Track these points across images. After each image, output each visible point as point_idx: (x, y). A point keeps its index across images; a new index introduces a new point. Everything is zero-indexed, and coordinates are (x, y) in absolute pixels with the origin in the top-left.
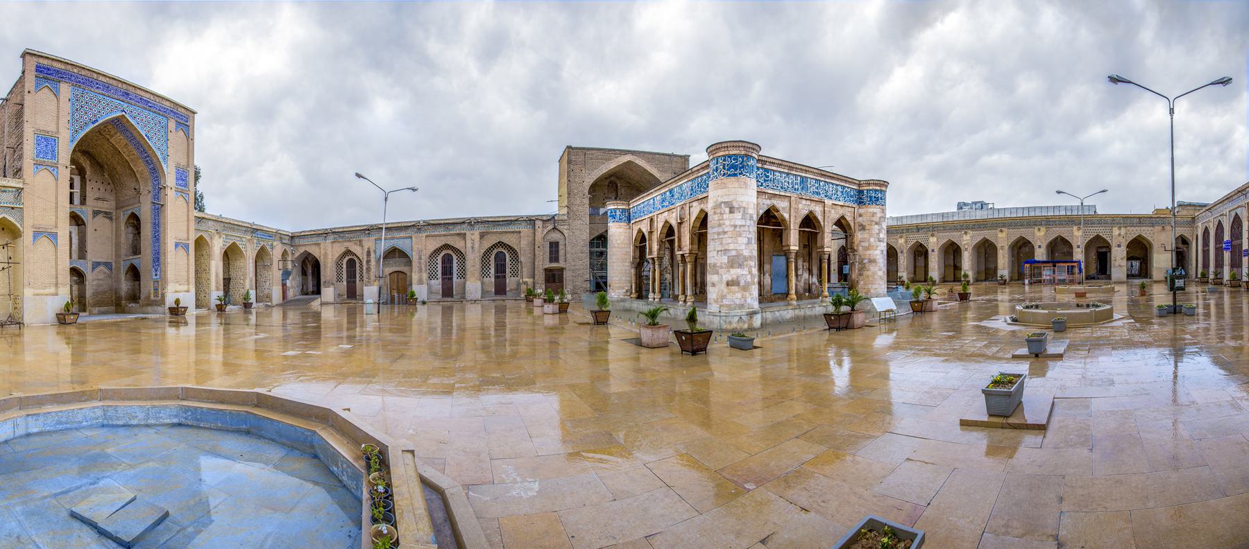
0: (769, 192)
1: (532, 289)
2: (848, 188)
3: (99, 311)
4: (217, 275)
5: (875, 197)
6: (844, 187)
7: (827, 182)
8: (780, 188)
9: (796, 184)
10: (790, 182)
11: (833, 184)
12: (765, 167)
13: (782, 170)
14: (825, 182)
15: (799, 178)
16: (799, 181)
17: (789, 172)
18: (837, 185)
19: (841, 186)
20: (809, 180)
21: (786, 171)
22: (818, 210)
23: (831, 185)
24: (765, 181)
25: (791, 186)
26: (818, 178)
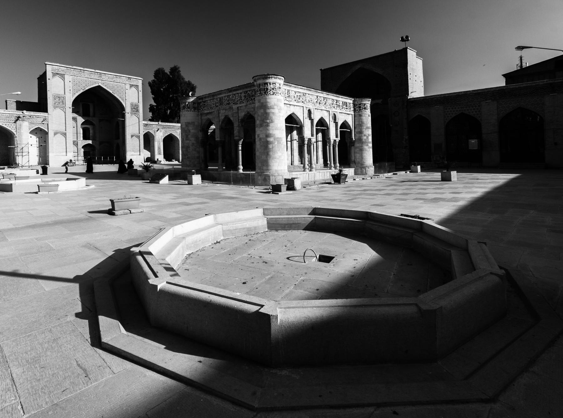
0: (206, 112)
1: (72, 162)
2: (249, 91)
4: (159, 148)
6: (247, 92)
7: (234, 95)
8: (210, 109)
9: (217, 103)
10: (214, 103)
11: (238, 94)
12: (203, 100)
21: (212, 98)
22: (229, 113)
24: (204, 107)
25: (214, 105)
26: (228, 94)
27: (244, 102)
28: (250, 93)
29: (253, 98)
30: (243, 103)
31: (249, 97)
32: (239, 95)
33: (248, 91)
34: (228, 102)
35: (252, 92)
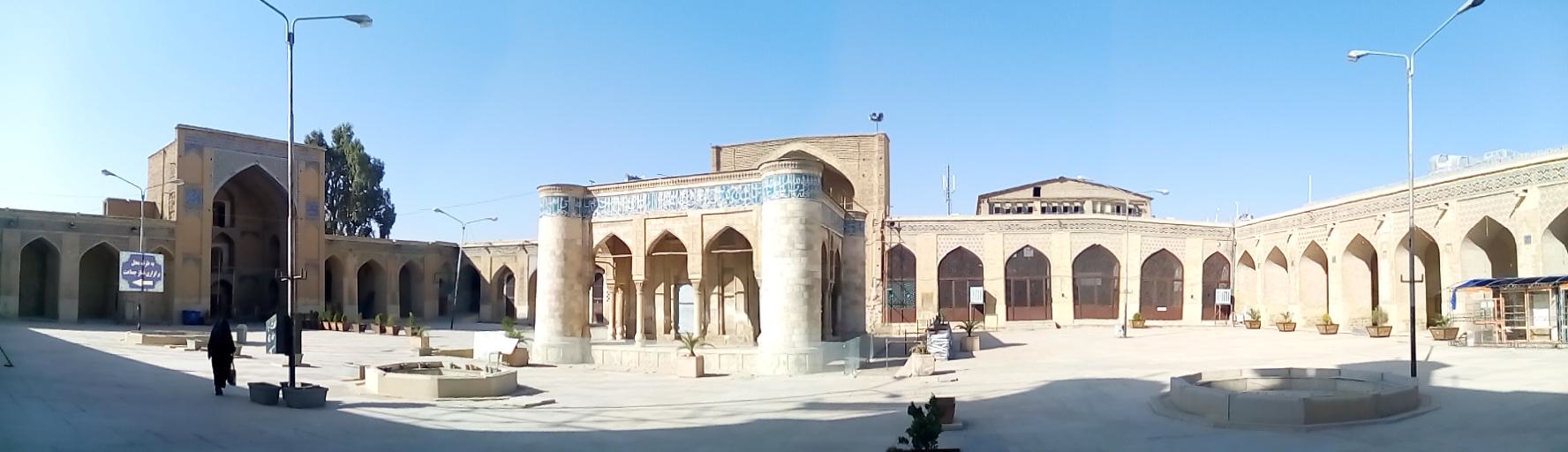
3: (216, 296)
5: (769, 189)
6: (727, 187)
7: (693, 189)
11: (703, 188)
13: (622, 193)
14: (689, 189)
15: (645, 195)
16: (645, 199)
17: (631, 192)
18: (713, 187)
19: (722, 186)
20: (661, 194)
21: (626, 192)
23: (701, 191)
25: (633, 208)
27: (720, 205)
28: (736, 189)
29: (746, 199)
30: (717, 207)
31: (734, 196)
32: (707, 190)
33: (730, 185)
34: (674, 204)
35: (743, 187)
